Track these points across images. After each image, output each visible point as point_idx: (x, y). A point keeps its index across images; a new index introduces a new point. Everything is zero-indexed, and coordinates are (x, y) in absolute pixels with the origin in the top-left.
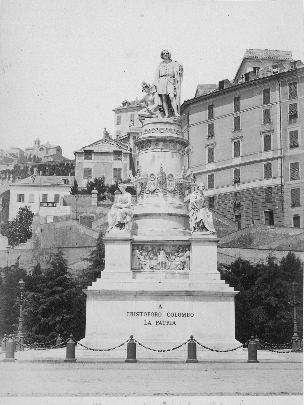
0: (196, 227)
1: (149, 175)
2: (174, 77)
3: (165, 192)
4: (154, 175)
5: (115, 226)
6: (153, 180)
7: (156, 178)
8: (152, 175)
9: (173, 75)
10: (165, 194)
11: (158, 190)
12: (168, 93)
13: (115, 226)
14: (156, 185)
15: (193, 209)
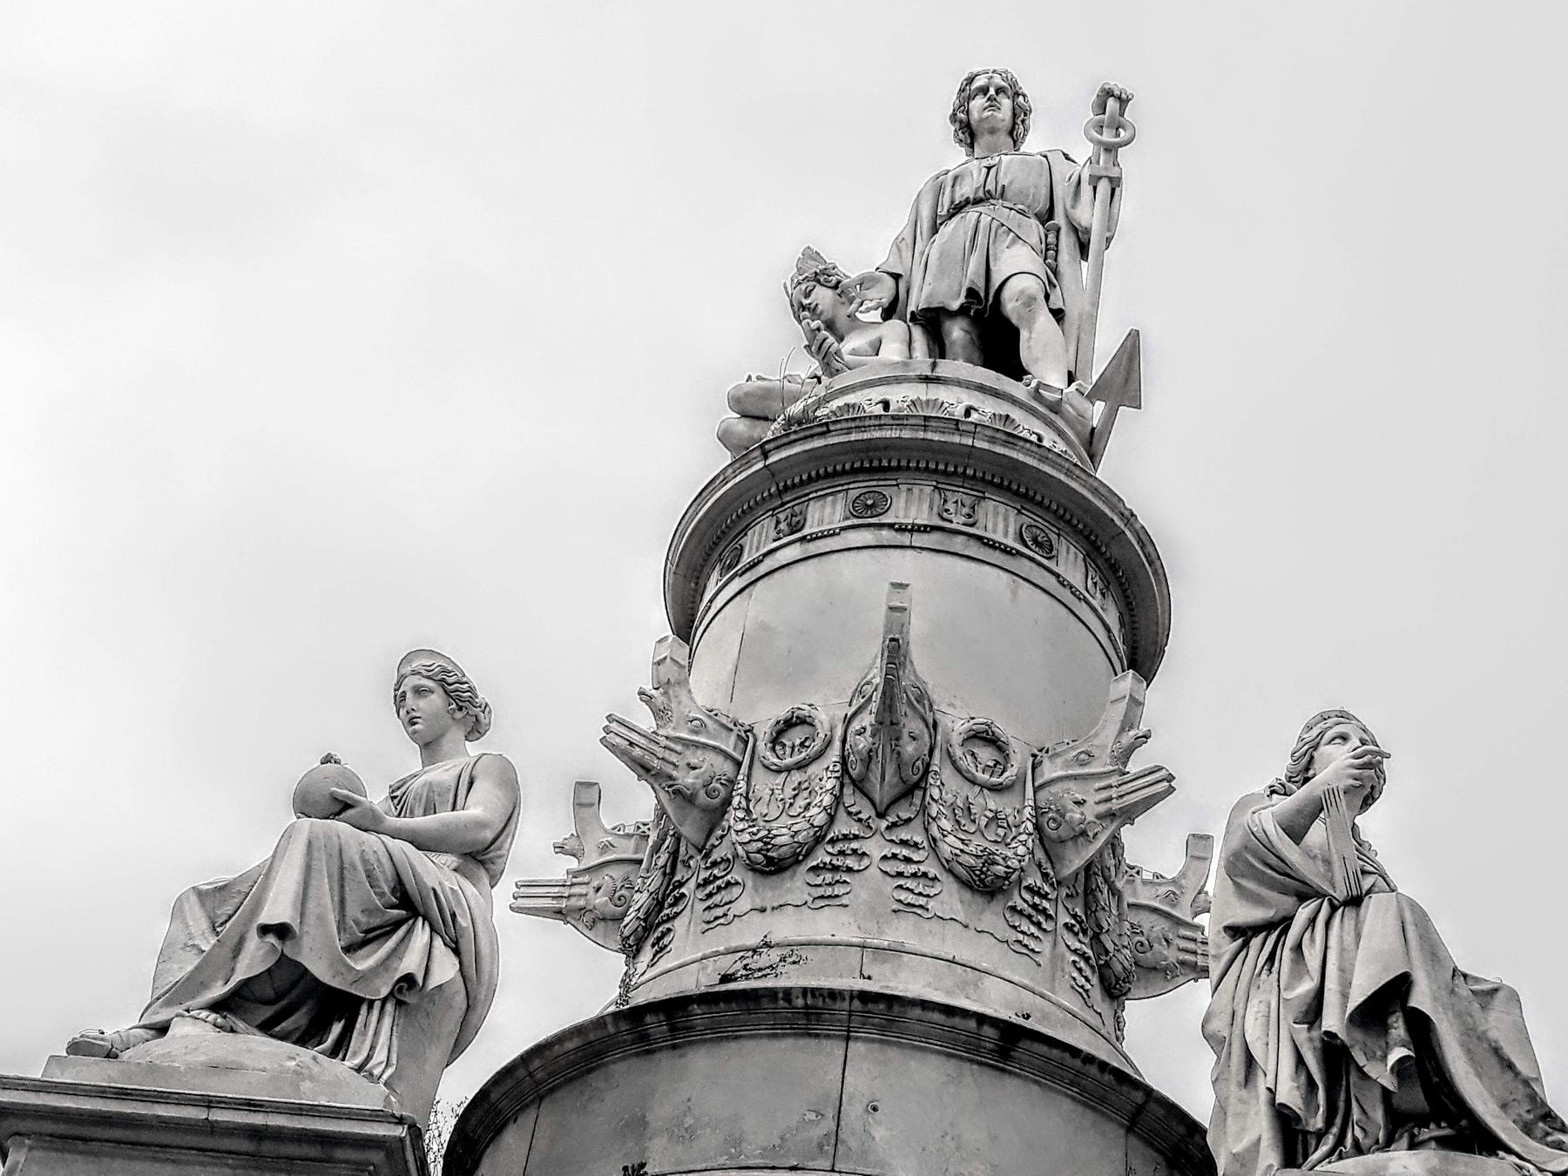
0: (1318, 1122)
1: (764, 731)
2: (1047, 216)
3: (912, 869)
4: (802, 721)
5: (215, 1007)
6: (801, 766)
7: (828, 743)
8: (789, 724)
9: (1042, 205)
10: (910, 884)
11: (839, 846)
12: (996, 282)
13: (215, 1007)
14: (827, 800)
15: (1255, 942)
